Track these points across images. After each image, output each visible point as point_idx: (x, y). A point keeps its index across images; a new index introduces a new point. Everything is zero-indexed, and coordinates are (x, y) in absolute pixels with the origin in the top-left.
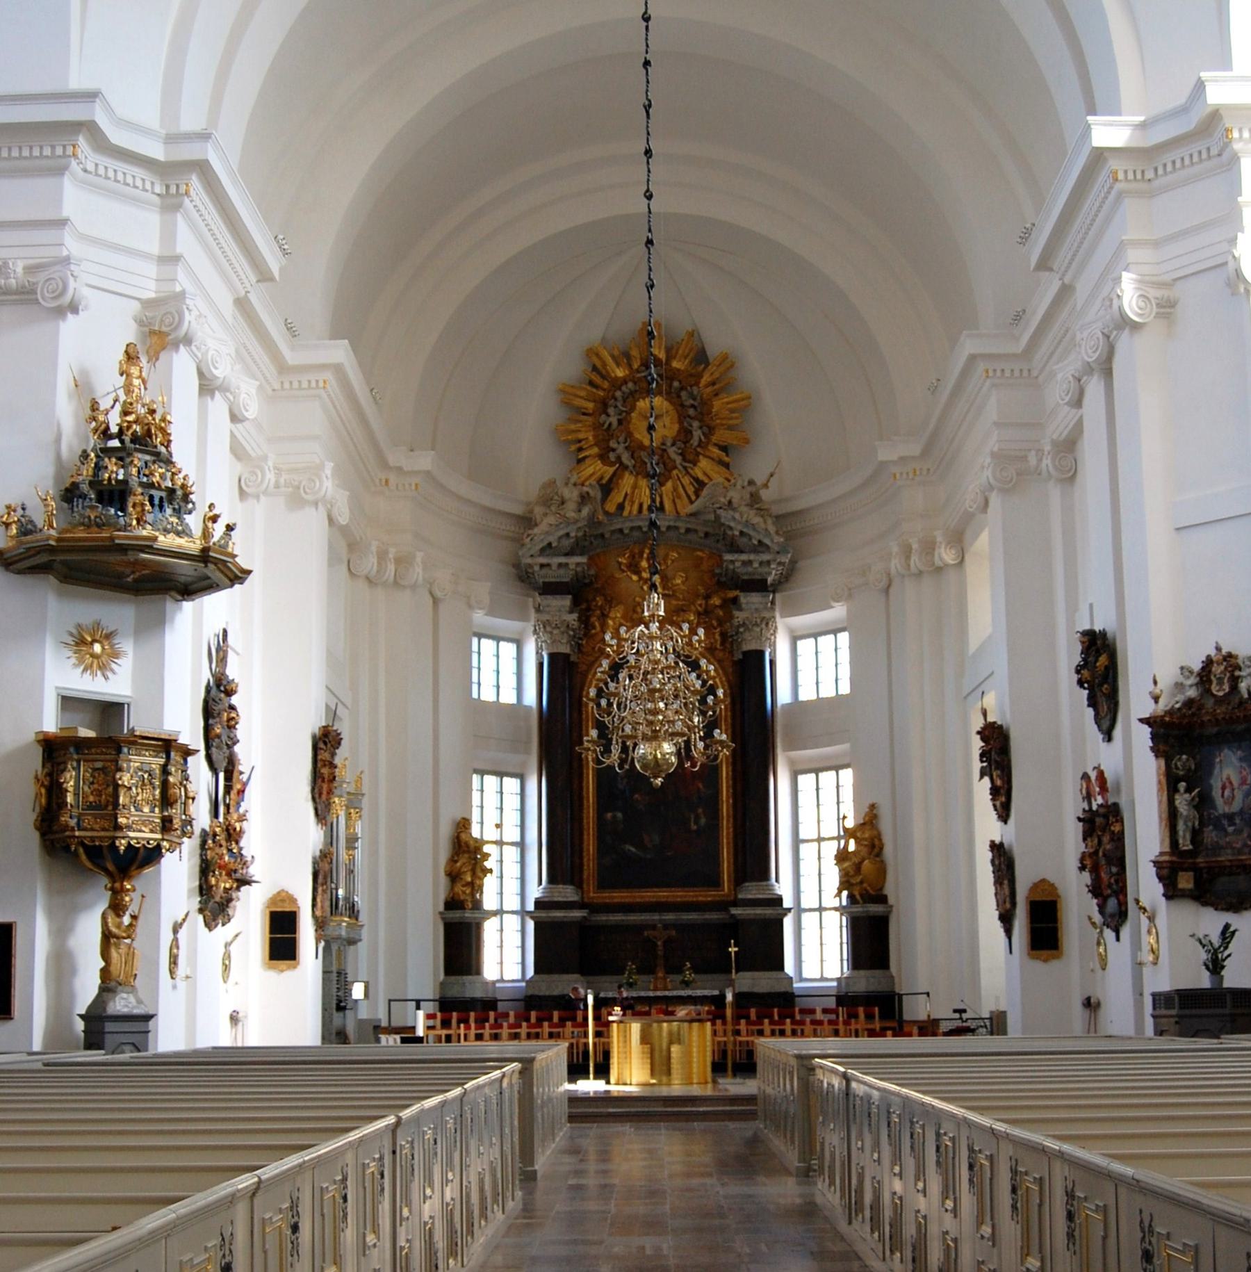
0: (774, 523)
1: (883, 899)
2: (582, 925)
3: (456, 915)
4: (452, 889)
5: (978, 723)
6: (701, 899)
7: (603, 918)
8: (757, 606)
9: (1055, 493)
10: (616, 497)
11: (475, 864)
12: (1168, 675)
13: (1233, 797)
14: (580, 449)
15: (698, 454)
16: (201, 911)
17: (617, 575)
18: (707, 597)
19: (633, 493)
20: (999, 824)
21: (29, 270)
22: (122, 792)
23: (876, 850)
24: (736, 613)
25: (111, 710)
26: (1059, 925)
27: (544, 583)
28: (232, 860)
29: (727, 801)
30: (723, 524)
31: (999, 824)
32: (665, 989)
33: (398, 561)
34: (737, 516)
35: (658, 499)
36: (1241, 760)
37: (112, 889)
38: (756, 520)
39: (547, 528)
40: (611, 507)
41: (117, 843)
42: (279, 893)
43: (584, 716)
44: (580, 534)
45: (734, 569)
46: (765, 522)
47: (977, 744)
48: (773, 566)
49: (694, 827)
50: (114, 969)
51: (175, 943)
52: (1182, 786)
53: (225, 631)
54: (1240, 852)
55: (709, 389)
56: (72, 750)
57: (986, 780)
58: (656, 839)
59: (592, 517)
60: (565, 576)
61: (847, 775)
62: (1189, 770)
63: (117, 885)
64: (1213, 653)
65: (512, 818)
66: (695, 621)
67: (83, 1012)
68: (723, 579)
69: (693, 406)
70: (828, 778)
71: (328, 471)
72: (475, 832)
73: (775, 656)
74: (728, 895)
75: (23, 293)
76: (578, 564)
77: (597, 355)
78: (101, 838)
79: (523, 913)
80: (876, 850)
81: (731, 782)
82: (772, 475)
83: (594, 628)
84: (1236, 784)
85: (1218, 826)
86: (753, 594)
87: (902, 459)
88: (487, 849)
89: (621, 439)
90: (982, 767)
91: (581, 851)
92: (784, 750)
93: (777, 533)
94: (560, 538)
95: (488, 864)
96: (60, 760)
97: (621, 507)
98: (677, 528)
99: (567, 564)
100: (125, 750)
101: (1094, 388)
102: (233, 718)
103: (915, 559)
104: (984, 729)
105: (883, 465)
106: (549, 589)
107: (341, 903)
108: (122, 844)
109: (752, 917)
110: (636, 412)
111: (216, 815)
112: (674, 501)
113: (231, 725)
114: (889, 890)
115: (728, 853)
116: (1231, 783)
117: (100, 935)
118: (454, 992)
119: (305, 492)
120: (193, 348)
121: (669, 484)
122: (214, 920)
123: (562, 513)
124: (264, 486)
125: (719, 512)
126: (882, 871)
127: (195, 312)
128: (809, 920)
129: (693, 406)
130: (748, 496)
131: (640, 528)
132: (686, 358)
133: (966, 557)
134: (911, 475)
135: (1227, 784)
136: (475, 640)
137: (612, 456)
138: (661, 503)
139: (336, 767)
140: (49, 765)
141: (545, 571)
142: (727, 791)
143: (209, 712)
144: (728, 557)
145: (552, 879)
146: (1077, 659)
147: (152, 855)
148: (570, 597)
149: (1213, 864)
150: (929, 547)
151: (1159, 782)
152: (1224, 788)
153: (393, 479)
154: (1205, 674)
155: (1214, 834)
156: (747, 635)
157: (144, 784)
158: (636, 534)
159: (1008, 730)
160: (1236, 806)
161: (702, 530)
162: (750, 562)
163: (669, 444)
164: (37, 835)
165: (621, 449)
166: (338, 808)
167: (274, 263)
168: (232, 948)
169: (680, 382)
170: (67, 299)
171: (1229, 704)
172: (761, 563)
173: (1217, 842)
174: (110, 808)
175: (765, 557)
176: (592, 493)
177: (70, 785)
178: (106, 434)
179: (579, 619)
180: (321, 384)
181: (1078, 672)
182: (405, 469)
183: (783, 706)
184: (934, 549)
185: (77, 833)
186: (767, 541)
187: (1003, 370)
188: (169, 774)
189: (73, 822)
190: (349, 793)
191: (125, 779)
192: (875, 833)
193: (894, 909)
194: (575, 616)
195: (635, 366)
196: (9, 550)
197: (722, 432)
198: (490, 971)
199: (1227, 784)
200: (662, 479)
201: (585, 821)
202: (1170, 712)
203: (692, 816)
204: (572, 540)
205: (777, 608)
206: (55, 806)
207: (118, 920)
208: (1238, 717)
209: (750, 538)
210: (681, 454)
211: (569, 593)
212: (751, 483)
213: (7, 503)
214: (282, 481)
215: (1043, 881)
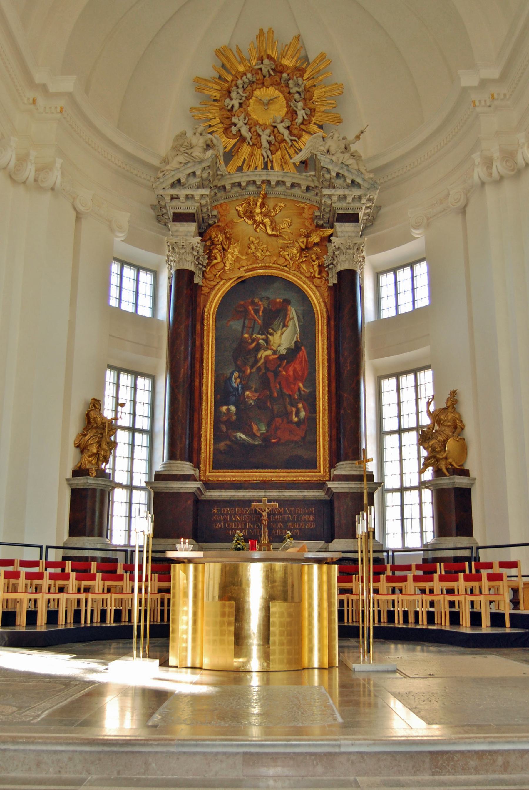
18: (308, 236)
29: (324, 398)
43: (205, 328)
49: (296, 419)
58: (263, 429)
66: (298, 254)
68: (321, 222)
69: (298, 93)
74: (325, 476)
81: (326, 382)
83: (216, 259)
89: (242, 116)
91: (200, 437)
92: (371, 358)
110: (253, 98)
112: (281, 165)
131: (254, 182)
132: (293, 57)
136: (115, 268)
137: (234, 130)
142: (323, 390)
163: (279, 120)
165: (240, 123)
169: (288, 75)
201: (204, 412)
203: (294, 410)
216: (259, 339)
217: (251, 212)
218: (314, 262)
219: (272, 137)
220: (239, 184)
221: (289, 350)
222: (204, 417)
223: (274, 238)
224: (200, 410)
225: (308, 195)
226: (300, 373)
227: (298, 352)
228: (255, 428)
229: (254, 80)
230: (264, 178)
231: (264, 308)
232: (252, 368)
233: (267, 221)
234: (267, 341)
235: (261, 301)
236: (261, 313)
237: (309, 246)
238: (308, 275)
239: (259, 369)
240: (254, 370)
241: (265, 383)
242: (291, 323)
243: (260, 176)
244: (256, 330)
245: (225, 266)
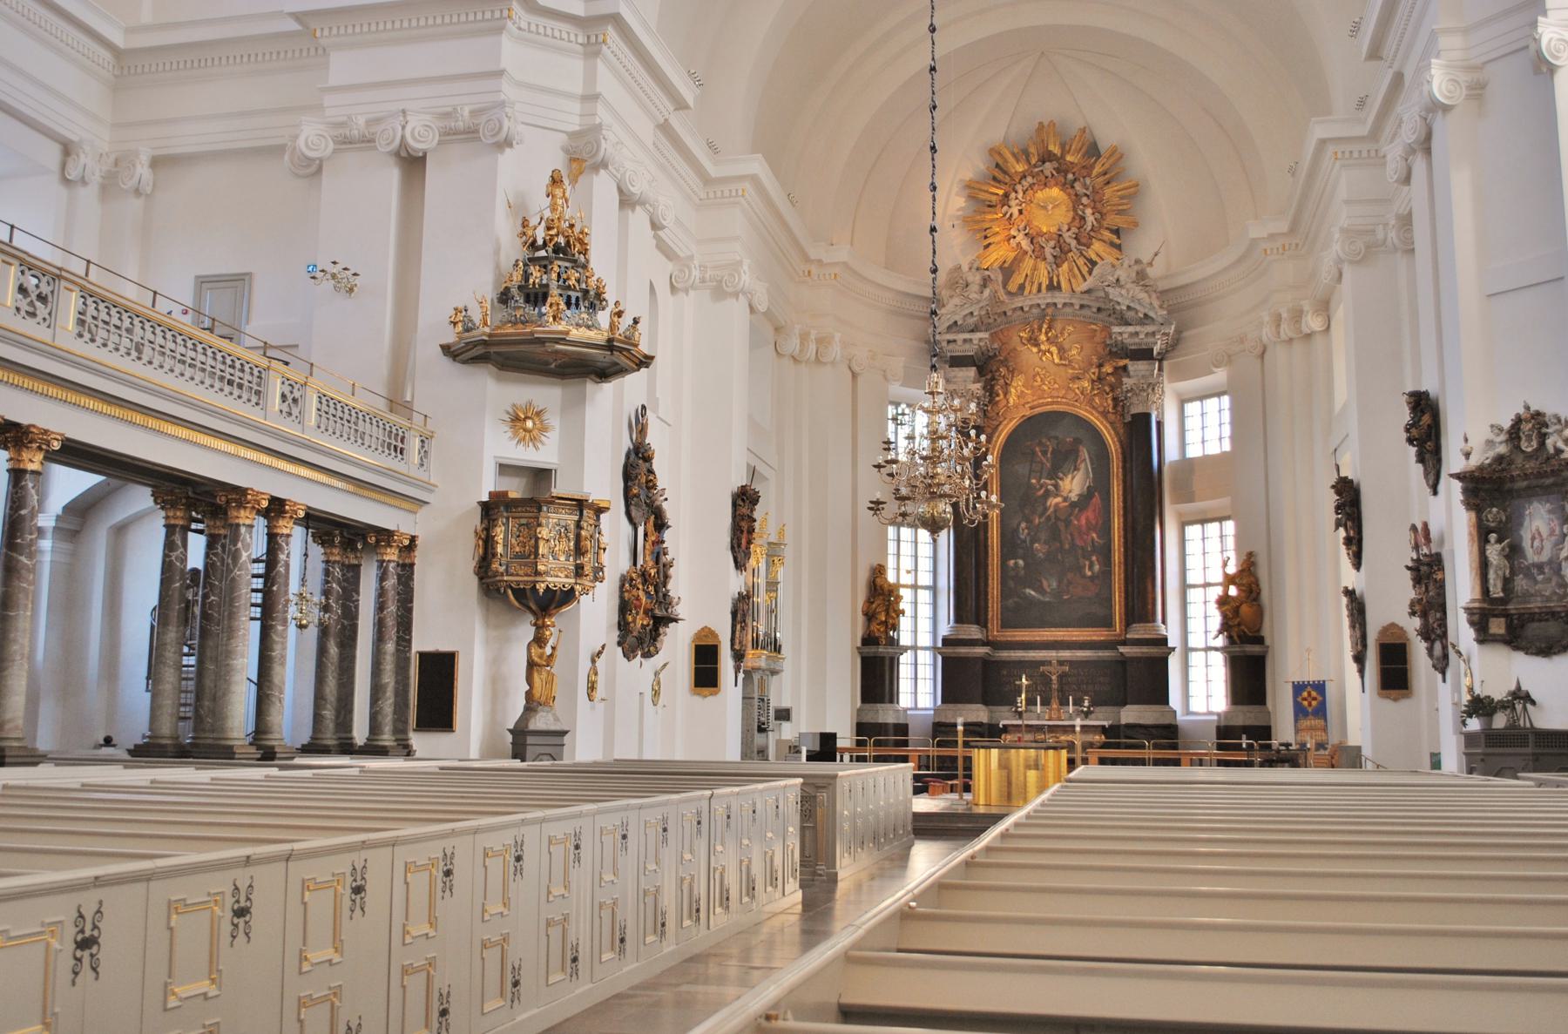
0: (1158, 298)
1: (1260, 640)
2: (986, 663)
3: (871, 650)
4: (869, 627)
5: (1333, 479)
6: (1095, 638)
7: (1005, 655)
8: (1143, 373)
10: (1018, 279)
11: (889, 605)
13: (1542, 548)
14: (986, 237)
15: (1091, 238)
16: (619, 644)
17: (1019, 349)
18: (1100, 366)
19: (1033, 274)
20: (1354, 571)
21: (474, 113)
22: (541, 543)
23: (1254, 595)
24: (1125, 380)
25: (541, 476)
26: (1408, 666)
27: (951, 357)
28: (649, 601)
29: (1119, 550)
30: (1111, 300)
32: (1059, 719)
33: (820, 341)
34: (1124, 292)
35: (1055, 279)
36: (1550, 512)
37: (535, 624)
38: (1143, 295)
39: (952, 310)
40: (1012, 287)
41: (538, 587)
42: (702, 629)
44: (983, 313)
45: (1123, 343)
46: (1150, 297)
47: (1331, 498)
48: (1158, 337)
49: (1089, 574)
50: (537, 693)
52: (1493, 537)
53: (644, 407)
54: (1549, 599)
55: (1101, 179)
56: (502, 508)
58: (1054, 584)
59: (994, 294)
60: (969, 350)
61: (1229, 527)
62: (1501, 521)
63: (540, 622)
64: (1521, 411)
65: (925, 564)
67: (511, 727)
68: (1114, 350)
70: (1213, 528)
71: (745, 268)
72: (891, 577)
73: (1163, 418)
74: (1120, 635)
75: (469, 132)
76: (980, 340)
77: (1000, 154)
78: (526, 582)
79: (934, 648)
80: (1254, 595)
81: (1122, 533)
82: (1156, 255)
83: (998, 395)
85: (1528, 575)
86: (1140, 362)
87: (1272, 237)
88: (902, 592)
90: (1337, 519)
93: (1161, 307)
94: (965, 316)
95: (902, 606)
96: (495, 517)
97: (1022, 287)
98: (1072, 304)
99: (971, 340)
100: (545, 509)
102: (651, 480)
103: (1284, 326)
104: (1337, 483)
105: (1254, 241)
106: (957, 362)
107: (761, 638)
108: (541, 587)
109: (1140, 655)
111: (635, 564)
113: (650, 485)
115: (1120, 596)
116: (1539, 534)
117: (526, 664)
118: (869, 718)
119: (727, 286)
120: (610, 167)
121: (1065, 266)
122: (633, 651)
123: (966, 294)
124: (691, 282)
125: (1107, 289)
126: (1260, 613)
128: (1196, 659)
129: (1086, 195)
130: (1134, 275)
131: (1039, 305)
133: (1333, 324)
134: (1281, 250)
135: (1537, 536)
138: (1059, 282)
139: (755, 521)
140: (486, 521)
141: (951, 346)
142: (1119, 540)
143: (628, 475)
144: (1116, 329)
145: (959, 618)
147: (568, 596)
148: (974, 368)
149: (1522, 611)
150: (1298, 315)
151: (1470, 534)
152: (1533, 539)
153: (814, 270)
154: (1514, 433)
155: (1524, 582)
156: (1134, 400)
157: (560, 537)
158: (1035, 311)
159: (1358, 485)
160: (1545, 557)
161: (1095, 305)
162: (1137, 334)
164: (474, 580)
166: (759, 556)
168: (661, 676)
170: (503, 135)
171: (1537, 459)
172: (1147, 334)
173: (1527, 590)
174: (532, 557)
175: (1150, 329)
176: (992, 277)
177: (500, 538)
179: (984, 388)
180: (740, 193)
181: (1407, 430)
182: (825, 261)
183: (1171, 463)
184: (1301, 317)
185: (505, 578)
186: (1152, 314)
187: (1351, 152)
188: (582, 528)
189: (502, 569)
190: (769, 544)
191: (544, 532)
192: (1252, 579)
193: (1270, 650)
194: (979, 385)
195: (1033, 162)
196: (454, 344)
197: (1112, 217)
198: (905, 700)
199: (1537, 536)
200: (1058, 260)
203: (1087, 563)
204: (975, 319)
205: (1165, 374)
206: (490, 556)
207: (540, 651)
208: (1546, 472)
209: (1137, 312)
210: (1075, 238)
211: (975, 365)
212: (1138, 262)
213: (455, 306)
214: (707, 276)
216: (1048, 485)
217: (1036, 340)
218: (1108, 394)
219: (1058, 249)
220: (1022, 308)
221: (1080, 495)
222: (990, 573)
223: (1062, 368)
224: (986, 566)
225: (1100, 316)
226: (1094, 522)
227: (1091, 499)
228: (1045, 583)
229: (1035, 181)
230: (1049, 301)
231: (1054, 450)
232: (1040, 517)
233: (1054, 349)
234: (1056, 486)
235: (1049, 440)
236: (1049, 455)
237: (1102, 376)
238: (1101, 409)
239: (1049, 518)
240: (1043, 520)
241: (1055, 535)
242: (1082, 466)
243: (1046, 298)
244: (1045, 474)
245: (1008, 402)
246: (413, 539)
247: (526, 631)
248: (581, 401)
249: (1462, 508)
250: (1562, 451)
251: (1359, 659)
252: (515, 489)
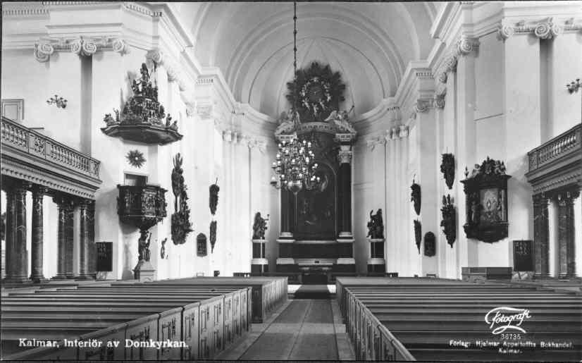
1: (382, 237)
5: (411, 184)
9: (438, 112)
12: (471, 168)
31: (417, 215)
36: (495, 194)
47: (411, 191)
51: (163, 248)
52: (474, 203)
57: (413, 202)
64: (486, 160)
84: (492, 201)
85: (485, 216)
101: (451, 76)
114: (384, 234)
127: (164, 54)
146: (441, 163)
154: (483, 167)
160: (491, 209)
164: (118, 217)
167: (193, 40)
178: (138, 92)
202: (471, 179)
215: (430, 232)
246: (94, 201)
247: (137, 235)
248: (156, 151)
249: (464, 193)
250: (500, 173)
251: (418, 244)
252: (129, 183)
